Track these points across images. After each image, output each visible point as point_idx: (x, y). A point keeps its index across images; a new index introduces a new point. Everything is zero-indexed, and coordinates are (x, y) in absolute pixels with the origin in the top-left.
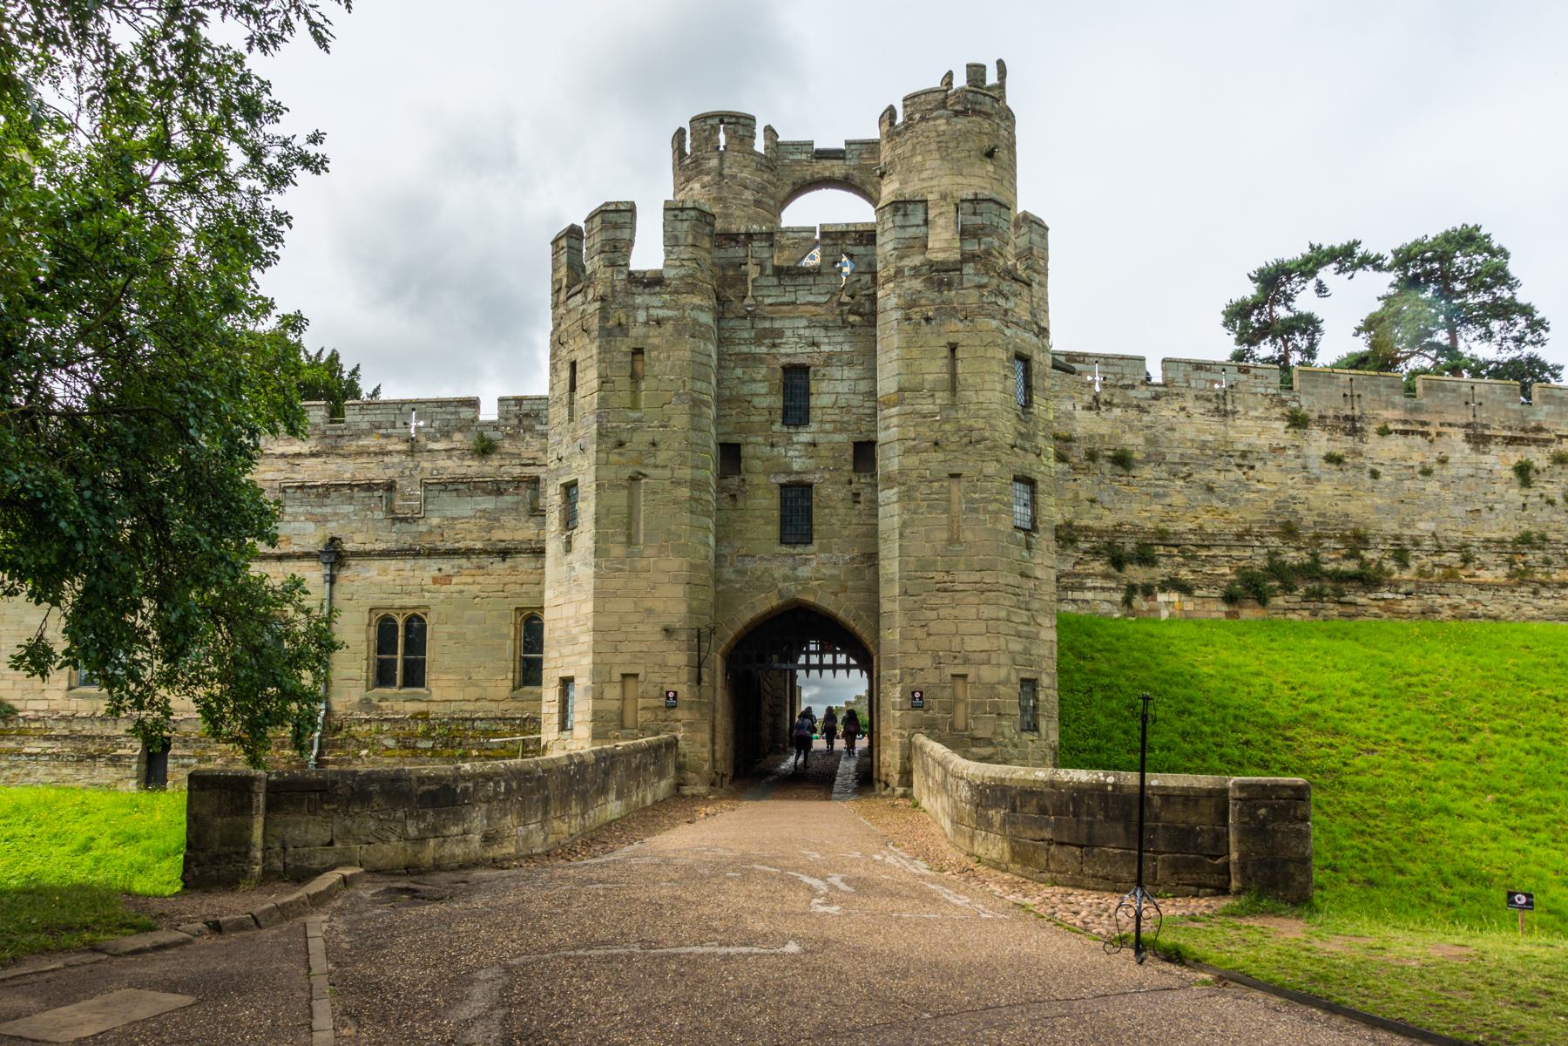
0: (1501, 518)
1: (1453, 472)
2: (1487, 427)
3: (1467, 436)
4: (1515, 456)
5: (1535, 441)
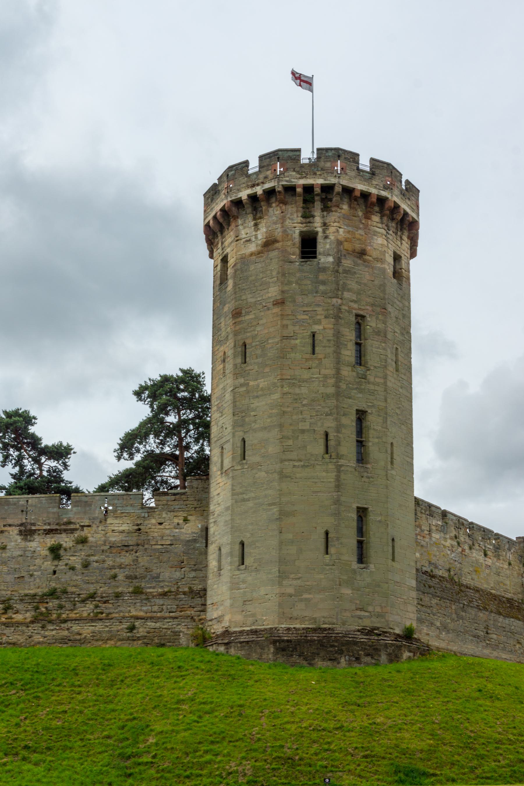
0: (38, 580)
1: (8, 555)
2: (34, 524)
3: (20, 531)
4: (50, 541)
5: (65, 530)
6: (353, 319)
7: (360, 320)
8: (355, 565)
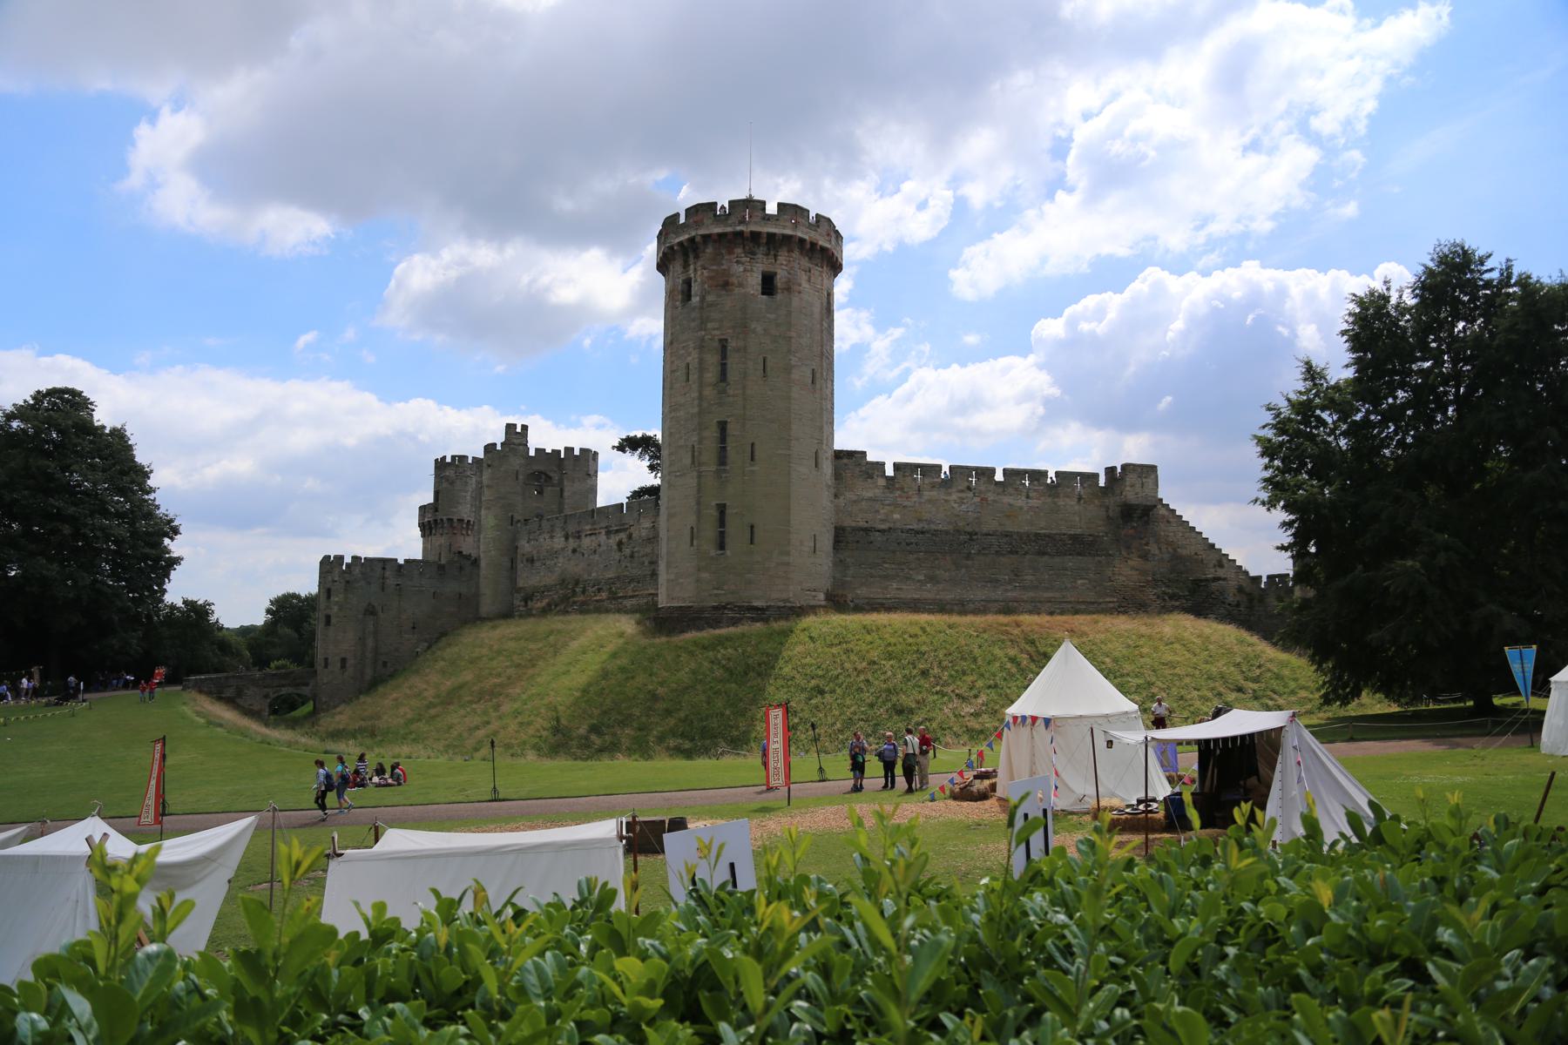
6: (716, 344)
7: (723, 344)
8: (713, 553)
